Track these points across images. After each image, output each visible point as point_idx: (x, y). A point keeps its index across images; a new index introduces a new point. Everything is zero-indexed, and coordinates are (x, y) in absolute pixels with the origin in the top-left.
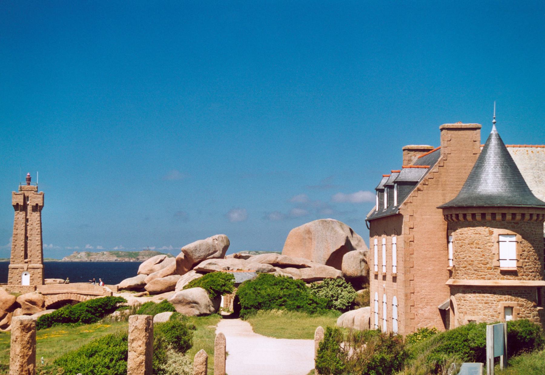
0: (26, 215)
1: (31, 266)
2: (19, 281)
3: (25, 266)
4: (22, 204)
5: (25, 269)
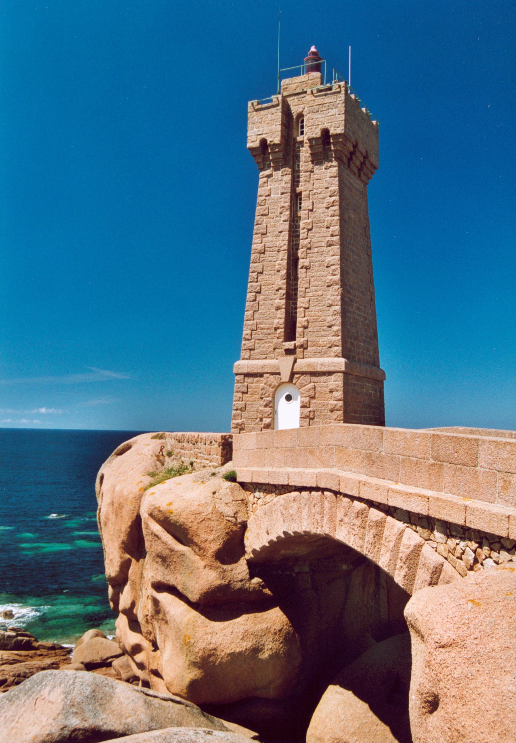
0: (295, 181)
1: (302, 364)
2: (267, 421)
3: (285, 364)
4: (277, 140)
5: (285, 377)
